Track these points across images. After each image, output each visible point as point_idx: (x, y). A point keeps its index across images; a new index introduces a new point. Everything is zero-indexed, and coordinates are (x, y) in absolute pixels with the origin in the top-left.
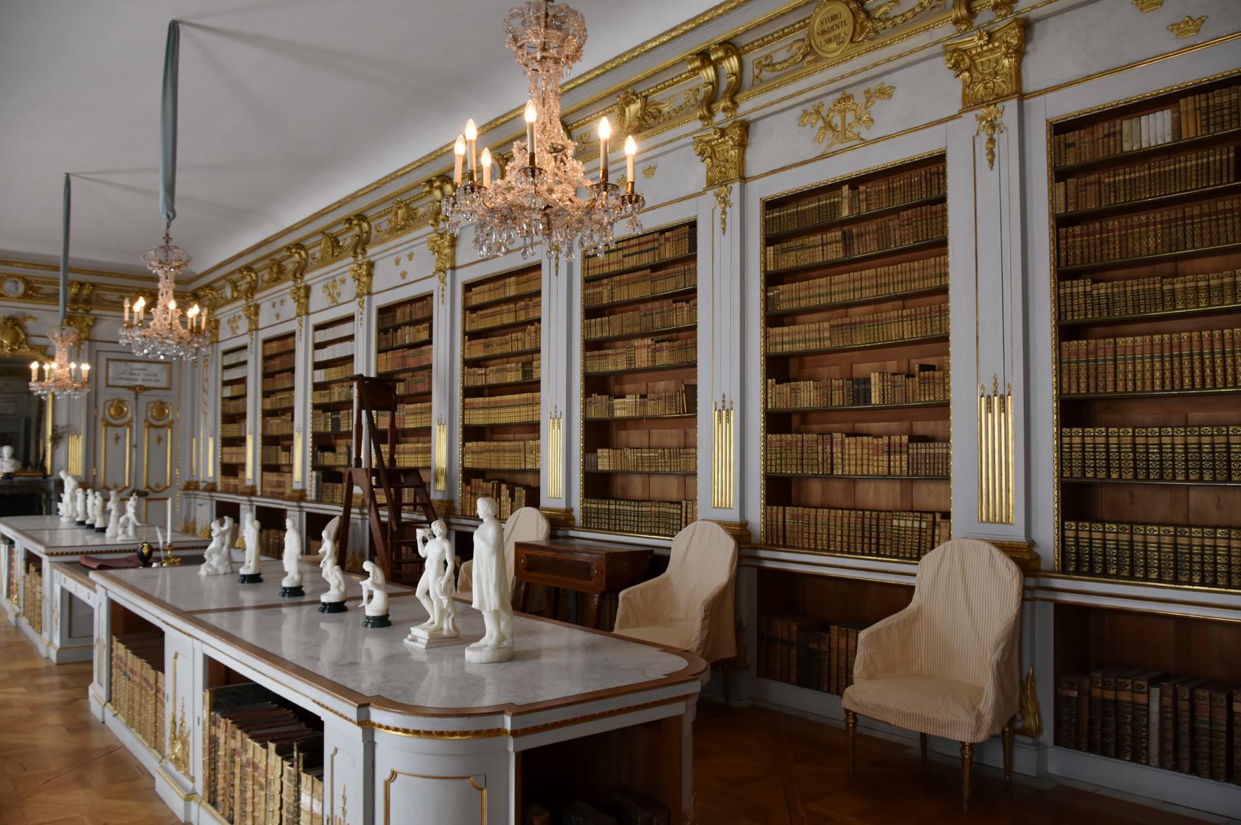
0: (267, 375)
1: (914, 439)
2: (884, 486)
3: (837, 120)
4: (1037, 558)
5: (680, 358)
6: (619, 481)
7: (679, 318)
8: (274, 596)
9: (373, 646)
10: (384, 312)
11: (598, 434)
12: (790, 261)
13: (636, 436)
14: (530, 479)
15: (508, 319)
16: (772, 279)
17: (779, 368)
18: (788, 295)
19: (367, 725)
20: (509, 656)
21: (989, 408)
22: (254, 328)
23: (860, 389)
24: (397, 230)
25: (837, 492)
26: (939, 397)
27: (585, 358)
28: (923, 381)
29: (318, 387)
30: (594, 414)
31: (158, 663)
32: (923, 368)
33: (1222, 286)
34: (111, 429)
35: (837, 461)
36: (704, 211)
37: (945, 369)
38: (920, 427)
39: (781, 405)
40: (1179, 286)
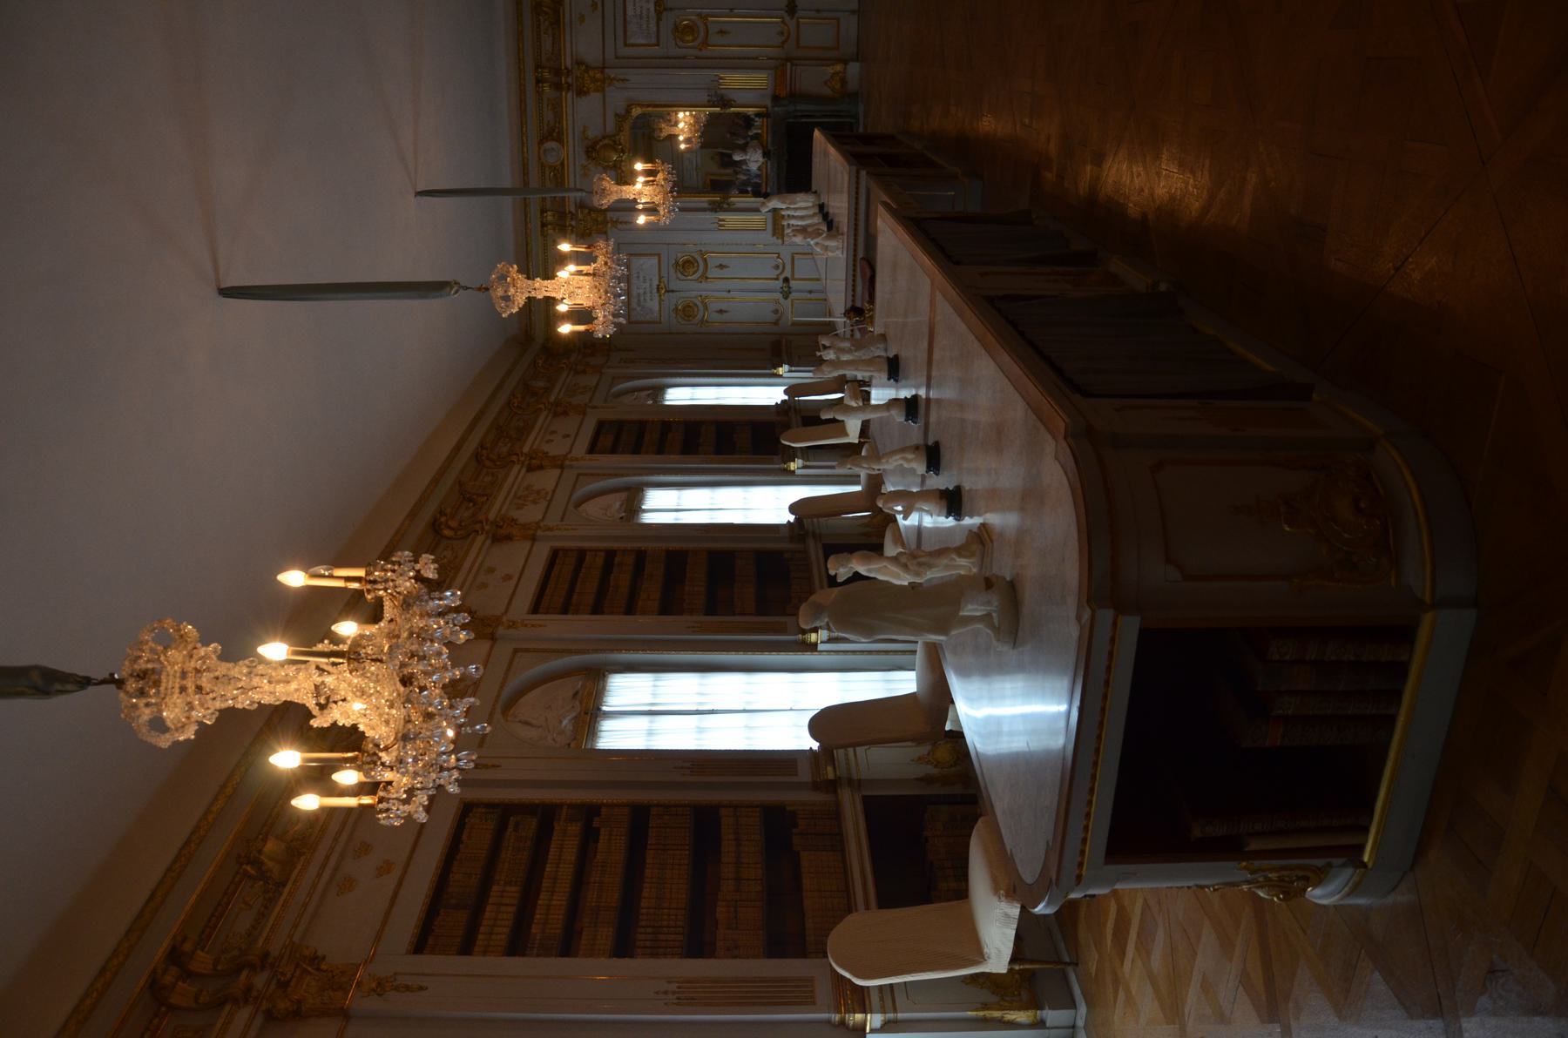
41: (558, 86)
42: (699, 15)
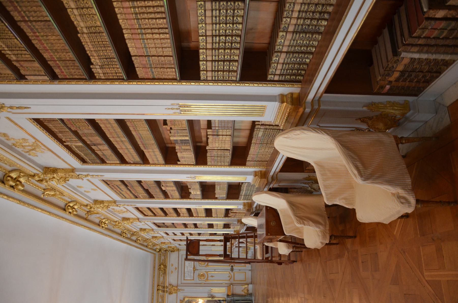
10: (159, 226)
27: (173, 199)
30: (200, 197)
34: (209, 279)
40: (82, 24)
41: (164, 291)
42: (206, 271)
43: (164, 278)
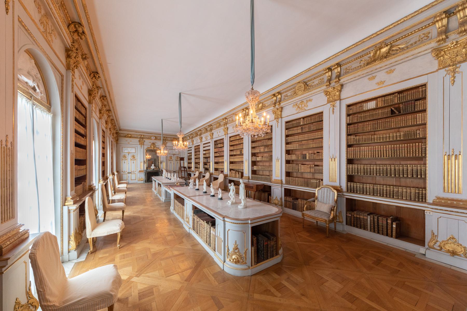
0: (195, 152)
1: (315, 166)
2: (308, 174)
3: (300, 106)
4: (342, 189)
5: (269, 150)
6: (257, 172)
7: (269, 142)
8: (202, 193)
9: (220, 203)
10: (215, 141)
11: (254, 163)
12: (290, 133)
13: (261, 164)
14: (241, 171)
15: (237, 143)
16: (287, 136)
17: (288, 152)
18: (290, 139)
19: (224, 221)
20: (246, 207)
21: (332, 160)
22: (193, 144)
23: (304, 157)
24: (217, 127)
25: (299, 175)
26: (321, 158)
28: (317, 155)
29: (204, 154)
30: (253, 160)
31: (183, 205)
32: (318, 152)
33: (386, 137)
35: (300, 169)
36: (274, 124)
37: (322, 153)
38: (316, 163)
39: (289, 159)
43: (169, 140)
